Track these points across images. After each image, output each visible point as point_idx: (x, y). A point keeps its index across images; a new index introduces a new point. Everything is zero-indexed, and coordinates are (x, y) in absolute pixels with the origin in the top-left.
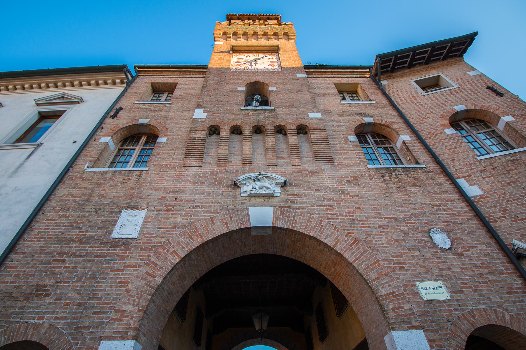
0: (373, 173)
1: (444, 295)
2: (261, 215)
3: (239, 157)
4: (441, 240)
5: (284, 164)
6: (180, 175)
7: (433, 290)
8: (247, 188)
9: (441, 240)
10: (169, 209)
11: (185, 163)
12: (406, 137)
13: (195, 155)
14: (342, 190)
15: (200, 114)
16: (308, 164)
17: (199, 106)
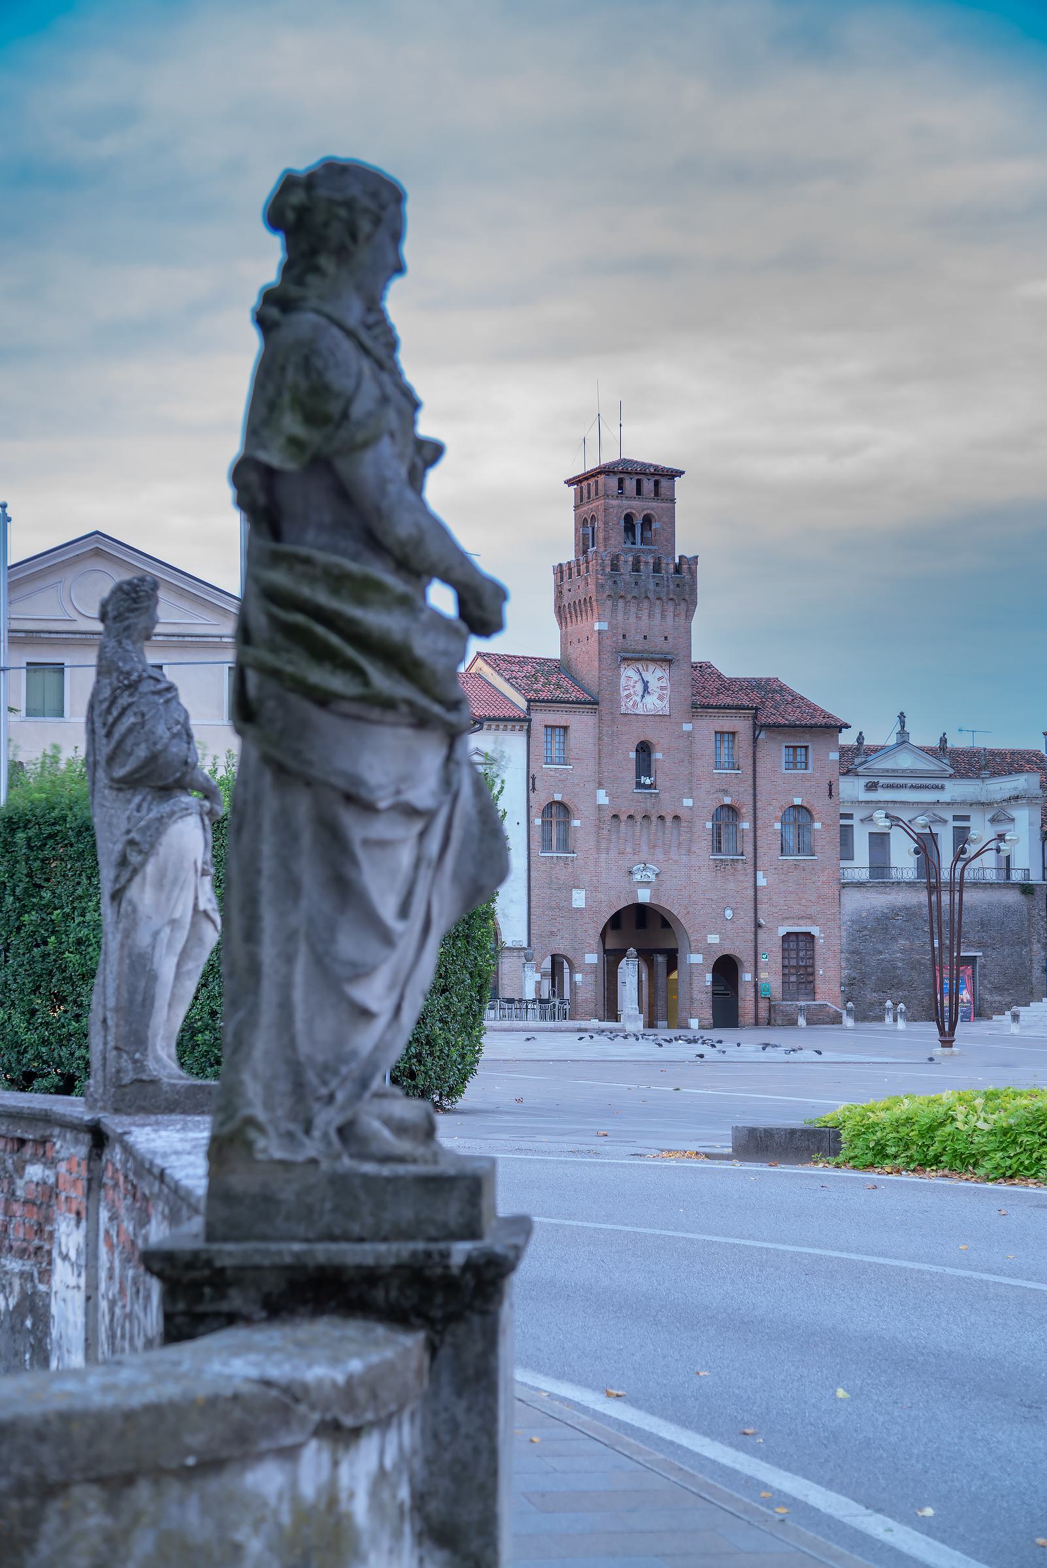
0: (711, 863)
1: (717, 941)
2: (644, 896)
3: (630, 845)
4: (729, 914)
5: (660, 855)
6: (597, 861)
7: (713, 939)
8: (638, 877)
9: (729, 914)
10: (596, 889)
11: (598, 851)
12: (746, 825)
13: (604, 845)
14: (690, 877)
15: (602, 798)
16: (674, 855)
17: (600, 785)
